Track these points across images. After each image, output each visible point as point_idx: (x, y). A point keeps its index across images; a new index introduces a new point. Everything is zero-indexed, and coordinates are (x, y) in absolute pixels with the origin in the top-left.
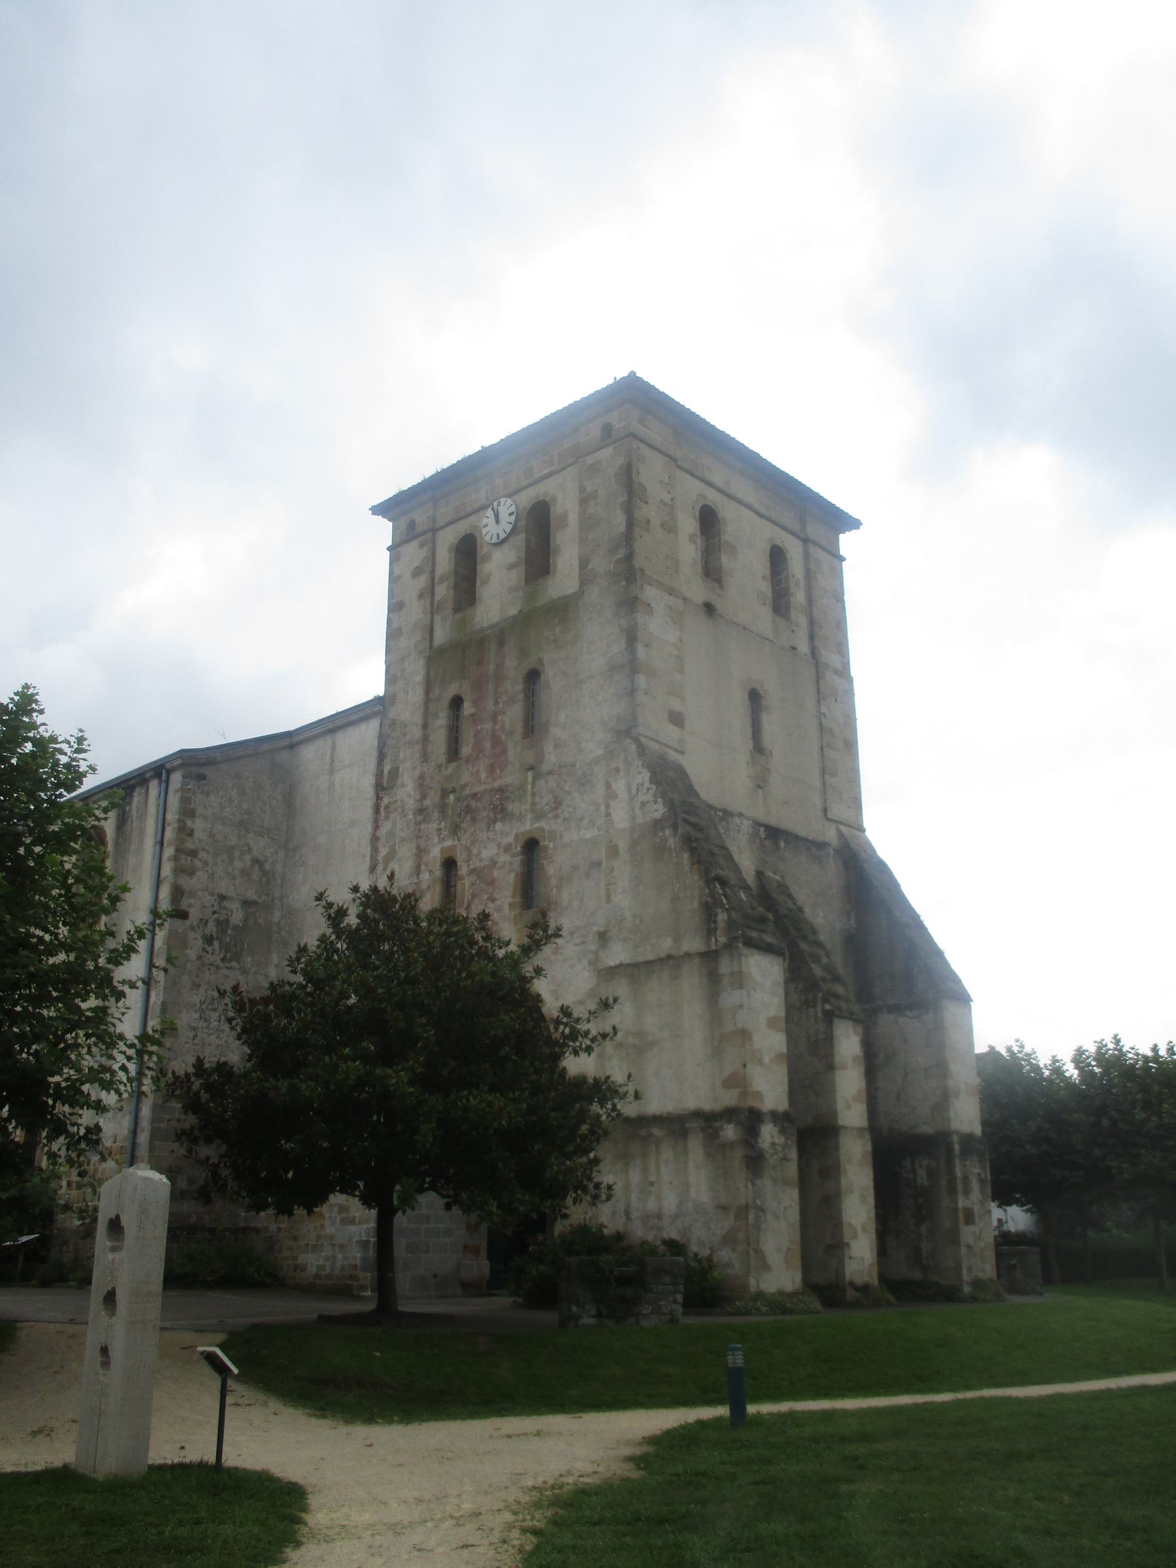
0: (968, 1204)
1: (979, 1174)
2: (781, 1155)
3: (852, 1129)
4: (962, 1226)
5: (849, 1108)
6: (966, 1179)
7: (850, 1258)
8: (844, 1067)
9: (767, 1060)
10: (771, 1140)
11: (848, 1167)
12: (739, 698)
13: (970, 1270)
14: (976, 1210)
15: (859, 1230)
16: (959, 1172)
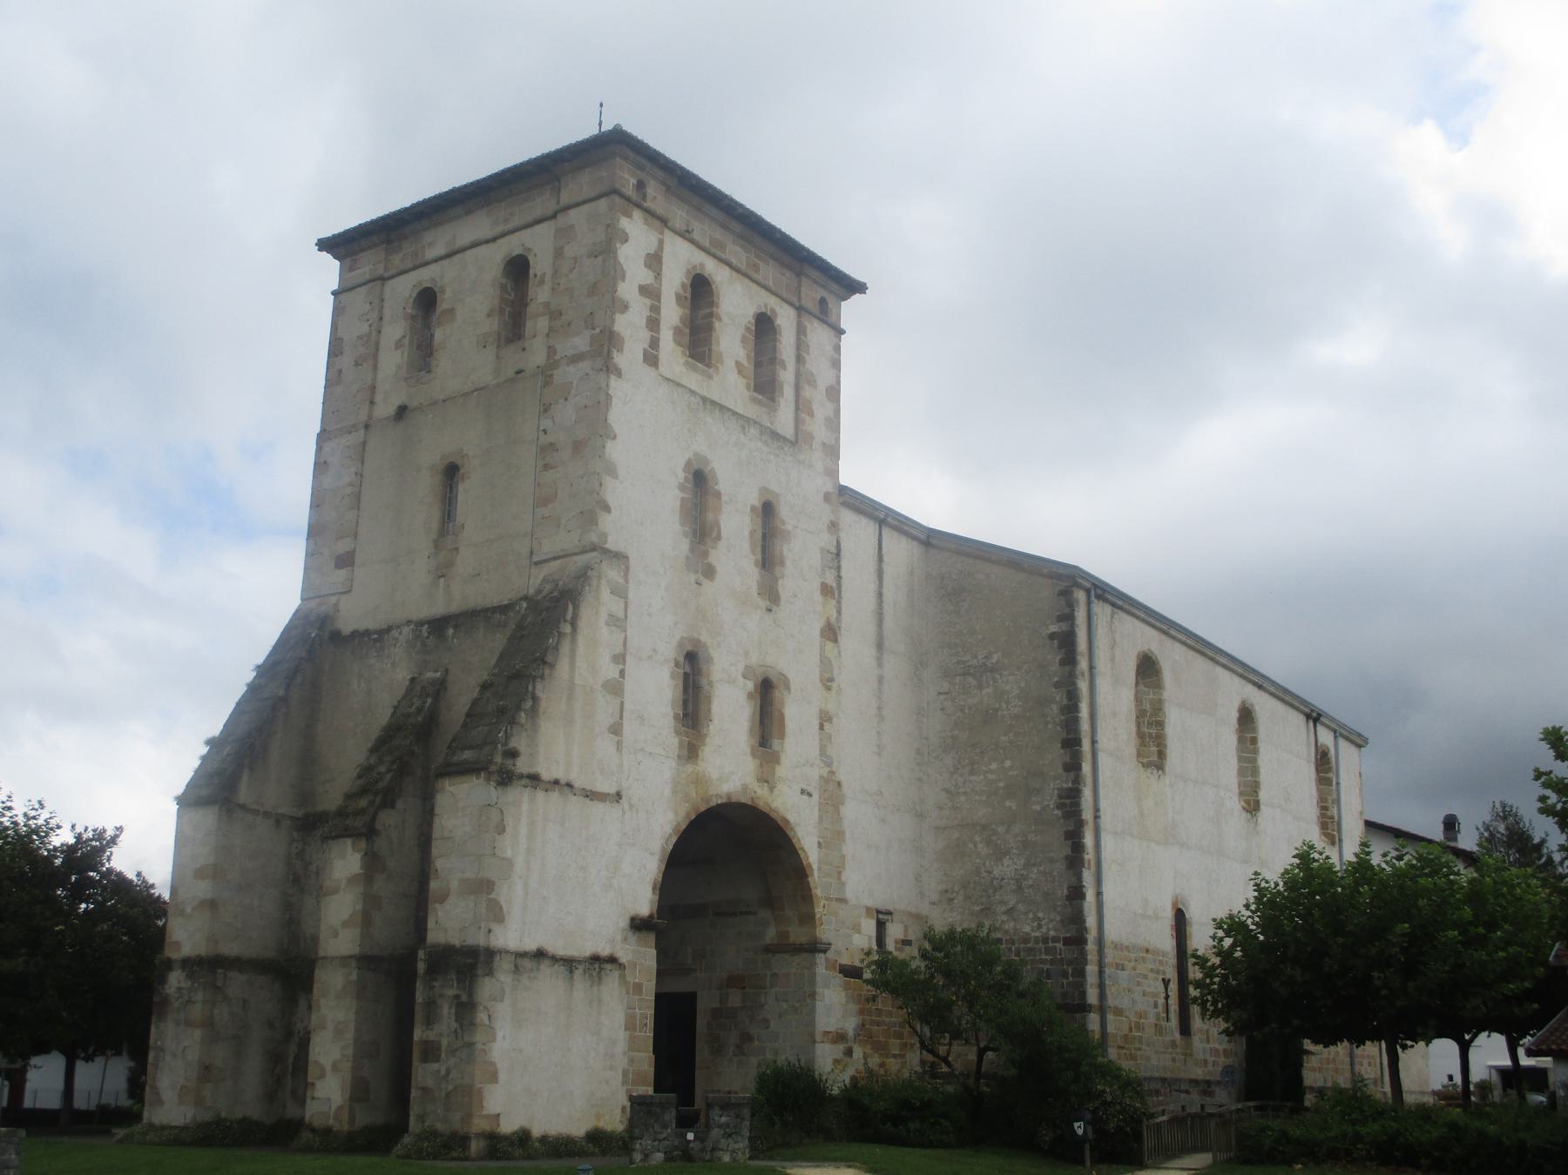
0: (431, 1035)
1: (457, 997)
2: (186, 998)
3: (333, 958)
4: (416, 1062)
5: (336, 935)
6: (431, 1005)
7: (313, 1098)
8: (336, 891)
9: (189, 910)
10: (177, 985)
11: (322, 1001)
12: (426, 485)
13: (421, 1118)
14: (444, 1042)
15: (329, 1068)
16: (420, 998)
